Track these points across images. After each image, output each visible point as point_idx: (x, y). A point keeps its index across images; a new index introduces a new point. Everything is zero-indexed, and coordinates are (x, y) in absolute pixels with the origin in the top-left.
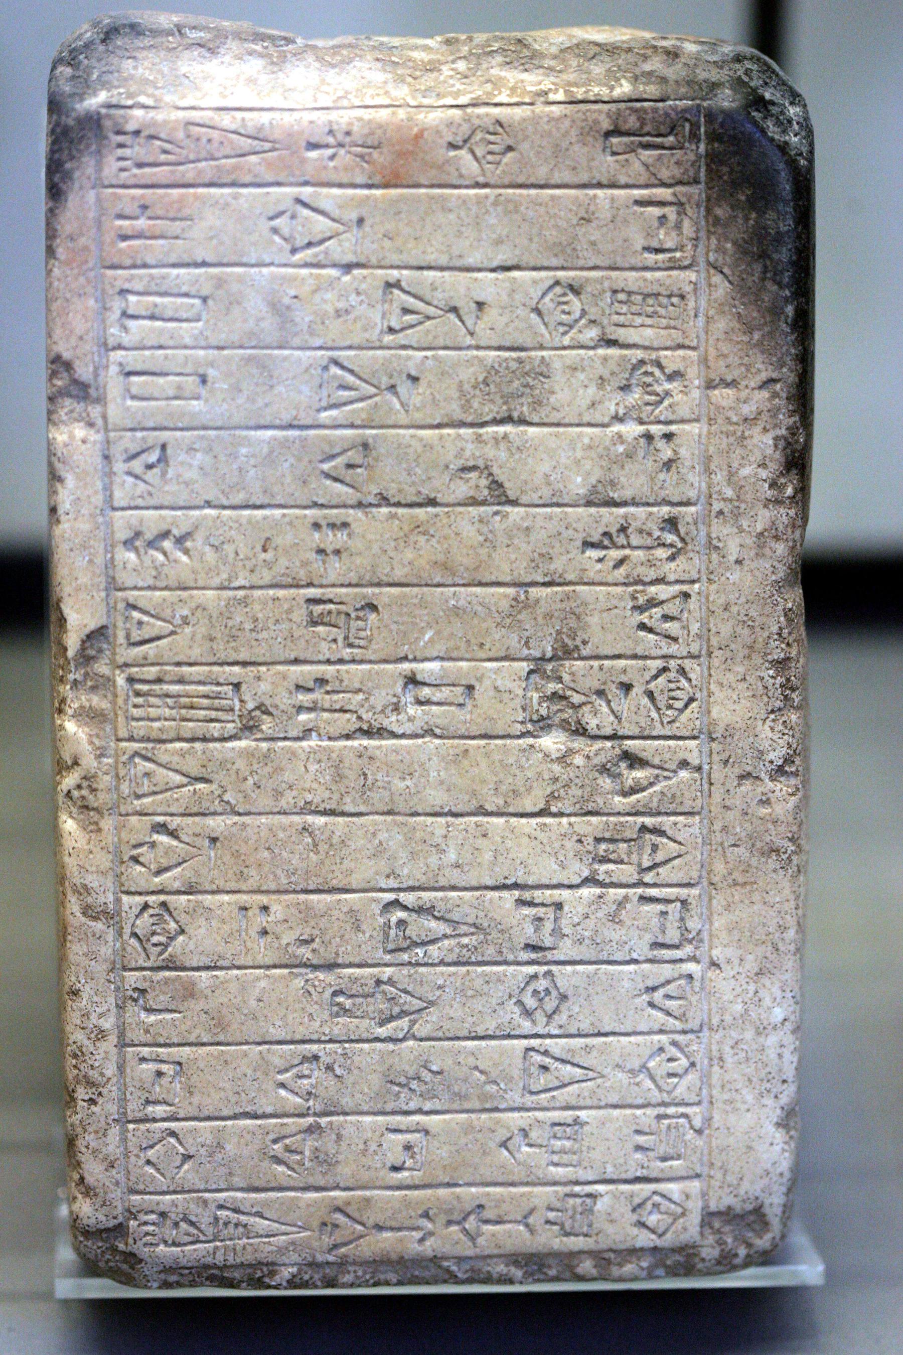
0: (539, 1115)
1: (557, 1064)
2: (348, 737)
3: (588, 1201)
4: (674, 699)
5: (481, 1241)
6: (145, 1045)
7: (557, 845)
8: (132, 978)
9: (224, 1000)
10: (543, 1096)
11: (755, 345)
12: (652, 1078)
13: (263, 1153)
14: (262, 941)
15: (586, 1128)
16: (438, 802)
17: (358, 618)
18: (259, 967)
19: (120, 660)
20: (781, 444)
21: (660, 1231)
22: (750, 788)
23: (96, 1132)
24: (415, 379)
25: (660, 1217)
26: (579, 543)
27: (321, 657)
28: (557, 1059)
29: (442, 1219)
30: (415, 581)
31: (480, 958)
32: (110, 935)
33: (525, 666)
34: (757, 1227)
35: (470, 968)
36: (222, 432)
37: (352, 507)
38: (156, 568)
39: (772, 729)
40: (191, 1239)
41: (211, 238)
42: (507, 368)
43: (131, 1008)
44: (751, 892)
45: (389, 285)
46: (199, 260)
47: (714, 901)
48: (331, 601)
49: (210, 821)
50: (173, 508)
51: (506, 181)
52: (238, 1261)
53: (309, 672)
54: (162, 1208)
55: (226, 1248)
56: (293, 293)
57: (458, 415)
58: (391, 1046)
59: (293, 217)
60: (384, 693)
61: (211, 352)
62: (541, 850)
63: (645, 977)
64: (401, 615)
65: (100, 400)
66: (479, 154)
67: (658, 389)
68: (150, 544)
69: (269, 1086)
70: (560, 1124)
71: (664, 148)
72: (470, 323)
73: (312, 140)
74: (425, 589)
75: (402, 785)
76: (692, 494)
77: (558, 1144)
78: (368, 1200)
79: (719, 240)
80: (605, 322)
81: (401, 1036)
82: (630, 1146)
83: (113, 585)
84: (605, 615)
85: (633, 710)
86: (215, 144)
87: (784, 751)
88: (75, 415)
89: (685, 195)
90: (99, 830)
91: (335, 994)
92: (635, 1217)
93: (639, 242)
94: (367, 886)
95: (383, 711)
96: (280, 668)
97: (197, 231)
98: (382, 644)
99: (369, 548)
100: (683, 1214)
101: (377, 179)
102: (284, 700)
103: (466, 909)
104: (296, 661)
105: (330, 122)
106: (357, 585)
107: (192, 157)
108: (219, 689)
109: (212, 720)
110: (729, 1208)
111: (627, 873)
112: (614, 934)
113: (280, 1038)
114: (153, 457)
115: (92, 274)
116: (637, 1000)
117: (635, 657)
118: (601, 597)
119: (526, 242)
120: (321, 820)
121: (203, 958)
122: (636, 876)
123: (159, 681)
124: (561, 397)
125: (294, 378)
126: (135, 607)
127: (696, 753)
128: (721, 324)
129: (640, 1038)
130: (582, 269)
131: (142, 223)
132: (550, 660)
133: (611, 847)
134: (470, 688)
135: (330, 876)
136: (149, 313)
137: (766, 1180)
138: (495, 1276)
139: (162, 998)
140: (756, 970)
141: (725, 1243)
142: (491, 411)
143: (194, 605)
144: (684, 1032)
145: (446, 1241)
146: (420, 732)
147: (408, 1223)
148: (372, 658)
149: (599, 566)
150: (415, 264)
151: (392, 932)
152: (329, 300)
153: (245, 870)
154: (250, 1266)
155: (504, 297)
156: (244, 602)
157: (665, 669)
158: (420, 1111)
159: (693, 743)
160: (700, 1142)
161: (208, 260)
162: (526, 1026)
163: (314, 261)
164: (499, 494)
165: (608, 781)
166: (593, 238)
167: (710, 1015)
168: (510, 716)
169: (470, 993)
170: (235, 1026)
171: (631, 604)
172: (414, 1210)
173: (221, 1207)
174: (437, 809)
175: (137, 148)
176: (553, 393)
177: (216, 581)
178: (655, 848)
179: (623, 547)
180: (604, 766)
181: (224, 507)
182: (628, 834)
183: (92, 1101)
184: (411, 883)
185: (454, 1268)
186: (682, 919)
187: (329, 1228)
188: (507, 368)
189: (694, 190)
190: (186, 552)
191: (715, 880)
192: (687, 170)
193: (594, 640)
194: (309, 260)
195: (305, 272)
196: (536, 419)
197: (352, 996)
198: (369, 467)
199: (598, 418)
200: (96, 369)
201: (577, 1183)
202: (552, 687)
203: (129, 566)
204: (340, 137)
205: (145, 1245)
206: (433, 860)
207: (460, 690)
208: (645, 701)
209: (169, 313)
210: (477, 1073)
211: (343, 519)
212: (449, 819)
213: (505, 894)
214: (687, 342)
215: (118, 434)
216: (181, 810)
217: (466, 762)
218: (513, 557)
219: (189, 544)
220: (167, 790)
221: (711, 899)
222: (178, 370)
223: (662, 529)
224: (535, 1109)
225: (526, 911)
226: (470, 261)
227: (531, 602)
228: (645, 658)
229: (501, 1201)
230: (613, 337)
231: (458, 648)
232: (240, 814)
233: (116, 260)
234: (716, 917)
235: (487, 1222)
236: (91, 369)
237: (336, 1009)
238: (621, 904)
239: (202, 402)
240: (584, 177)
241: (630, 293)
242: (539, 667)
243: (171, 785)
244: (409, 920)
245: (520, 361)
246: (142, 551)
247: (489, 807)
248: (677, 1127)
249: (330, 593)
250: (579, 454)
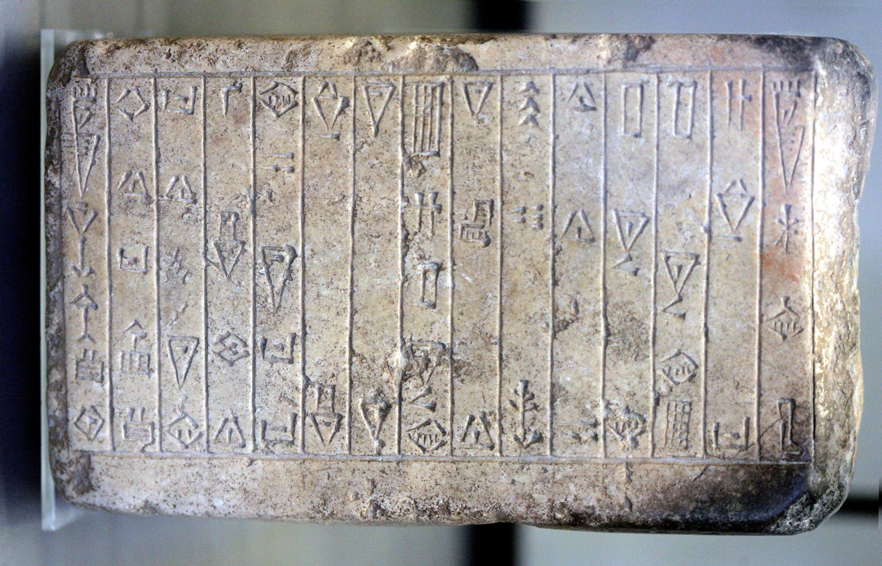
0: (156, 346)
1: (188, 359)
2: (403, 226)
3: (99, 378)
4: (425, 438)
5: (74, 307)
6: (205, 90)
7: (331, 361)
8: (249, 83)
9: (233, 143)
10: (168, 349)
11: (654, 495)
12: (178, 420)
13: (134, 166)
14: (271, 168)
15: (146, 377)
16: (360, 284)
17: (481, 234)
18: (254, 166)
19: (456, 79)
20: (590, 511)
21: (79, 424)
22: (366, 487)
23: (149, 58)
24: (635, 273)
25: (88, 424)
26: (527, 378)
27: (455, 209)
28: (192, 358)
29: (89, 282)
30: (504, 271)
31: (258, 309)
32: (277, 69)
33: (447, 341)
34: (80, 487)
35: (252, 303)
36: (603, 147)
37: (553, 231)
38: (515, 103)
39: (404, 502)
40: (78, 118)
41: (729, 142)
42: (642, 333)
43: (229, 82)
44: (299, 486)
45: (697, 257)
46: (715, 134)
47: (293, 463)
48: (492, 216)
49: (350, 136)
50: (554, 114)
51: (763, 335)
52: (64, 149)
53: (446, 202)
54: (99, 100)
55: (72, 141)
56: (693, 194)
57: (612, 301)
58: (202, 251)
59: (742, 196)
60: (431, 249)
61: (656, 140)
62: (328, 350)
63: (244, 417)
64: (483, 261)
65: (625, 69)
66: (781, 317)
67: (627, 432)
68: (531, 99)
69: (177, 171)
70: (149, 360)
71: (784, 436)
72: (672, 309)
73: (792, 209)
74: (499, 278)
75: (372, 260)
76: (558, 452)
77: (137, 359)
78: (102, 234)
79: (723, 472)
80: (671, 398)
81: (208, 257)
82: (134, 405)
83: (505, 75)
84: (480, 394)
85: (418, 412)
86: (790, 146)
87: (390, 510)
88: (616, 51)
89: (753, 451)
90: (345, 63)
91: (236, 215)
92: (88, 407)
93: (722, 420)
94: (306, 237)
95: (420, 249)
96: (449, 182)
97: (734, 133)
98: (463, 249)
99: (526, 242)
100: (89, 439)
101: (766, 251)
102: (428, 185)
103: (290, 301)
104: (453, 193)
105: (804, 221)
106: (502, 233)
107: (783, 130)
108: (436, 142)
109: (416, 137)
110: (93, 469)
111: (312, 406)
112: (273, 397)
113: (208, 179)
114: (587, 102)
115: (707, 64)
116: (229, 412)
117: (453, 413)
118: (492, 392)
119: (724, 347)
120: (349, 207)
121: (261, 129)
122: (310, 412)
123: (442, 103)
124: (623, 368)
125: (638, 194)
126: (490, 88)
127: (389, 452)
128: (668, 473)
129: (204, 413)
130: (706, 383)
131: (740, 97)
132: (452, 358)
133: (329, 396)
134: (434, 306)
135: (313, 213)
136: (681, 100)
137: (110, 493)
138: (51, 316)
139: (236, 102)
140: (248, 489)
141: (70, 466)
142: (614, 322)
143: (491, 127)
144: (208, 442)
145: (74, 285)
146: (406, 273)
147: (86, 260)
148: (455, 243)
149: (512, 391)
150: (711, 275)
151: (276, 253)
152: (688, 218)
153: (317, 158)
154: (60, 156)
155: (688, 332)
156: (492, 160)
157: (444, 433)
158: (159, 269)
159: (396, 450)
160: (136, 451)
161: (715, 140)
162: (213, 339)
163: (713, 209)
164: (559, 327)
165: (372, 395)
166: (725, 390)
167: (219, 458)
168: (415, 332)
169: (236, 303)
170: (216, 149)
171: (487, 411)
172: (95, 264)
173: (99, 138)
174: (356, 283)
175: (789, 94)
176: (625, 363)
177: (506, 142)
178: (328, 424)
179: (524, 407)
180: (382, 392)
181: (554, 148)
182: (337, 407)
183: (169, 56)
184: (308, 265)
185: (57, 289)
186: (281, 441)
187: (84, 208)
188: (642, 333)
189: (756, 457)
190: (526, 123)
191: (307, 463)
192: (769, 452)
193: (464, 387)
194: (714, 205)
195: (707, 202)
196: (608, 351)
197: (235, 226)
198: (579, 242)
199: (608, 392)
200: (646, 66)
201: (111, 370)
202: (434, 359)
203: (517, 85)
204: (794, 227)
205: (75, 89)
206: (322, 280)
207: (433, 299)
208: (424, 420)
209: (681, 114)
210: (183, 306)
211: (545, 225)
212: (349, 291)
213: (300, 327)
214: (657, 451)
215: (603, 79)
216: (357, 117)
217: (386, 302)
218: (519, 335)
219: (531, 124)
220: (371, 107)
221: (294, 460)
222: (644, 119)
223: (535, 432)
224: (159, 344)
225: (288, 340)
226: (712, 310)
227: (490, 346)
228: (452, 420)
229: (100, 320)
230: (661, 402)
231: (460, 298)
232: (354, 155)
233: (716, 80)
234: (283, 463)
235: (87, 311)
236: (646, 62)
237: (227, 215)
238: (292, 402)
239: (623, 134)
240: (765, 385)
241: (689, 414)
242: (447, 350)
243: (374, 110)
244: (284, 263)
245: (646, 342)
246: (527, 94)
247: (356, 317)
248: (146, 436)
249: (497, 216)
250: (585, 379)
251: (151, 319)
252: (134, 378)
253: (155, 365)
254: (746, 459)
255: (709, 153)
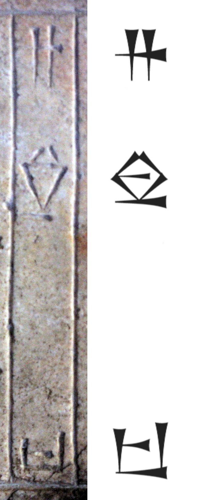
41: (36, 101)
46: (19, 92)
59: (53, 166)
93: (32, 436)
97: (42, 90)
115: (8, 7)
119: (33, 347)
130: (12, 391)
161: (19, 98)
163: (18, 182)
166: (35, 400)
194: (19, 177)
195: (10, 174)
233: (19, 26)
254: (61, 483)
255: (12, 115)
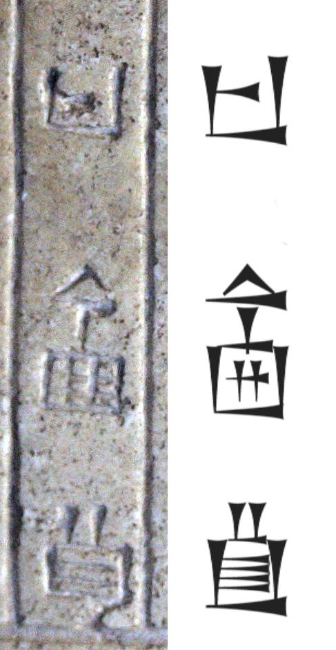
0: (141, 337)
15: (113, 420)
77: (87, 370)
82: (77, 498)
251: (130, 263)
252: (78, 425)
253: (137, 389)
